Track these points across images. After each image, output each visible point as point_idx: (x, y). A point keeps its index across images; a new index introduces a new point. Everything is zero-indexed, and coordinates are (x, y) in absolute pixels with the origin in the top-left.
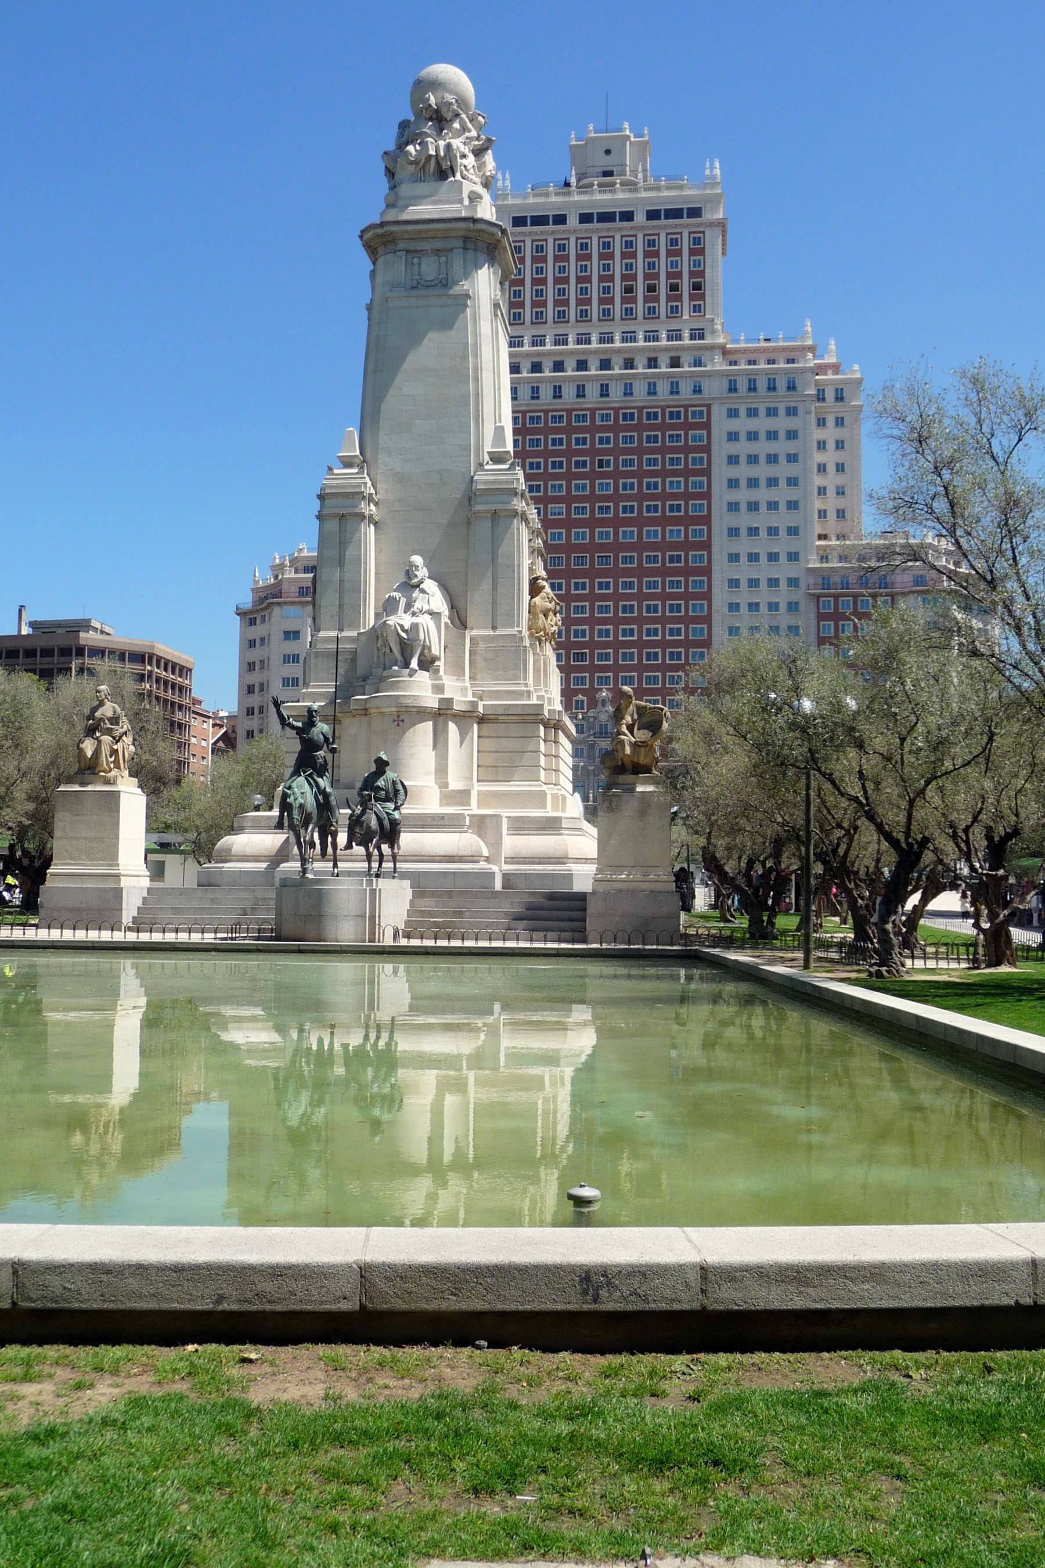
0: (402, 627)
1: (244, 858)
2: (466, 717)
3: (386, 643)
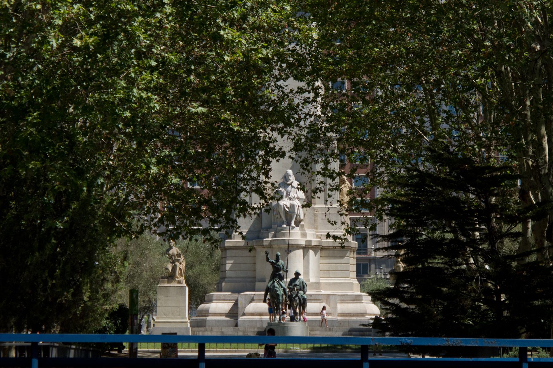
0: (286, 206)
1: (215, 315)
2: (319, 248)
3: (278, 213)
